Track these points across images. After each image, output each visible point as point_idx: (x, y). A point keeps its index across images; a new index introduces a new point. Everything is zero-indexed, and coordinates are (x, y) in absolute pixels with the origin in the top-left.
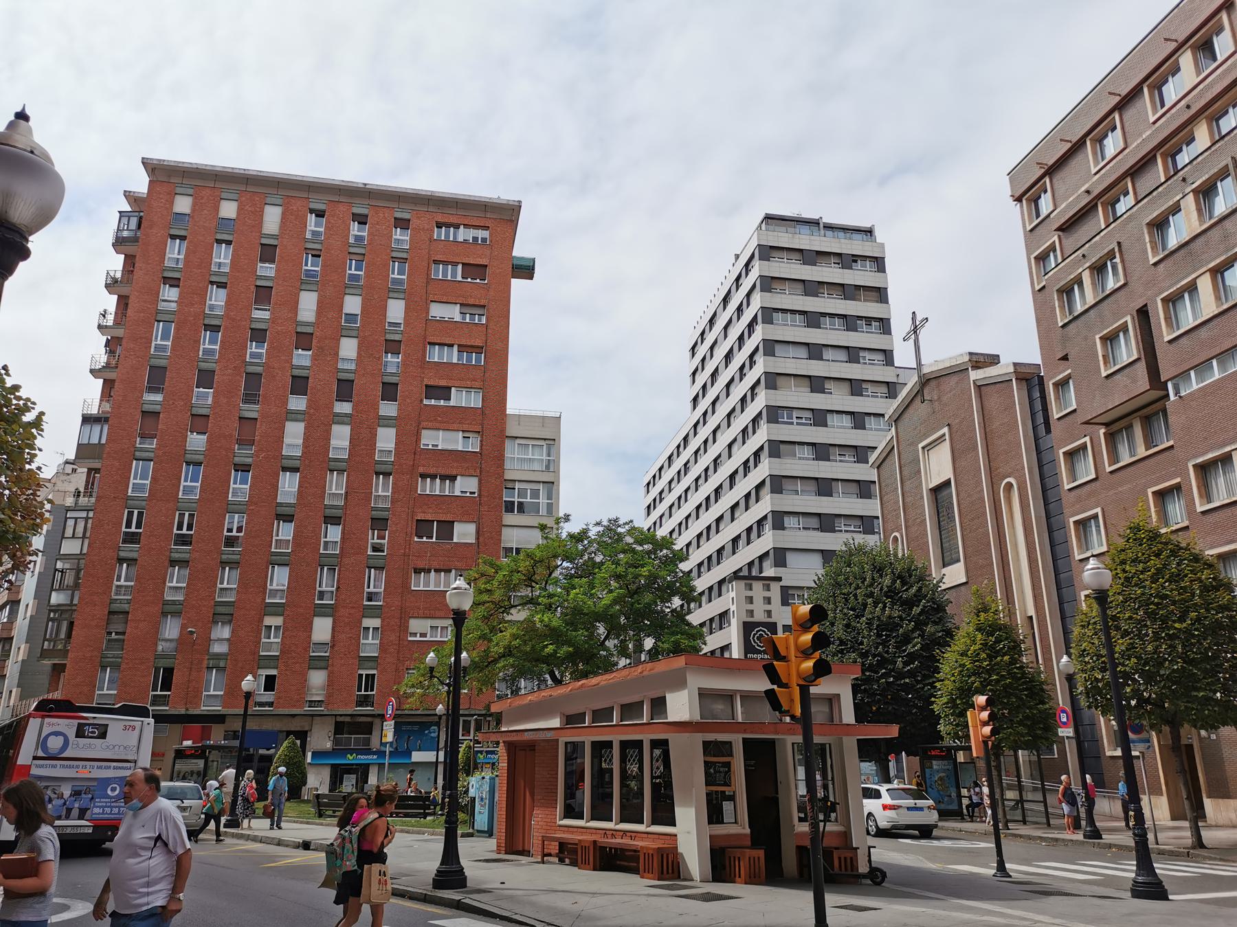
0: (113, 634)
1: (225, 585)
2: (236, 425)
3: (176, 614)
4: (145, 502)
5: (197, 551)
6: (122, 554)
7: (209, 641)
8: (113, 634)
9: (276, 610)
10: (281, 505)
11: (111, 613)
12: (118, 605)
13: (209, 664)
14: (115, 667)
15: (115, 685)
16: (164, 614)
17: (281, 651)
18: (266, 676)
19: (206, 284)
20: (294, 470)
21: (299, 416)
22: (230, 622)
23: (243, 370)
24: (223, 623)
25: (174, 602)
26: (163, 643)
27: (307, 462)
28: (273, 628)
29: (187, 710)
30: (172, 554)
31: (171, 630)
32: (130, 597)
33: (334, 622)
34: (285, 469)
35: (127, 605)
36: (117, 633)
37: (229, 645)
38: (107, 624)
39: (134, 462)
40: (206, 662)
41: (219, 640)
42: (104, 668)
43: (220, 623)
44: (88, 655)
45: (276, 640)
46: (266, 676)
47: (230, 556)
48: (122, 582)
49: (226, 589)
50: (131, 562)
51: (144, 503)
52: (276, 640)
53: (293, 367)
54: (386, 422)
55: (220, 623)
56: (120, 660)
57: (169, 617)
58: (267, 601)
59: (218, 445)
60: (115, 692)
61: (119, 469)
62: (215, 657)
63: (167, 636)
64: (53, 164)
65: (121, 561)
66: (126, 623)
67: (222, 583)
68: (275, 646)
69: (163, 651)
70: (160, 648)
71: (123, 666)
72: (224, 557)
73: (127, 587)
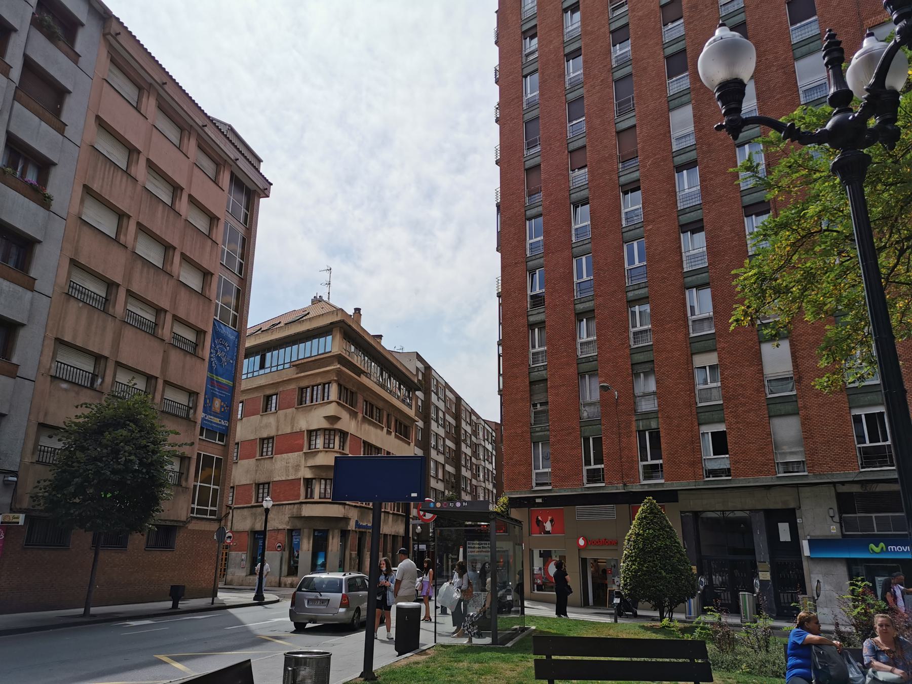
0: (538, 406)
1: (639, 328)
2: (615, 141)
3: (593, 373)
4: (543, 259)
5: (600, 296)
6: (532, 319)
7: (634, 398)
8: (538, 406)
9: (705, 345)
10: (684, 212)
11: (532, 383)
12: (536, 373)
13: (638, 426)
14: (546, 441)
15: (549, 462)
16: (581, 375)
17: (724, 398)
18: (712, 433)
19: (561, 13)
20: (690, 165)
21: (685, 99)
22: (652, 371)
23: (610, 79)
24: (646, 375)
25: (588, 360)
26: (587, 408)
27: (705, 148)
28: (707, 368)
29: (625, 485)
30: (577, 306)
31: (591, 391)
32: (546, 363)
33: (792, 346)
34: (679, 169)
35: (544, 372)
36: (541, 404)
37: (658, 398)
38: (531, 395)
39: (528, 222)
40: (634, 424)
41: (645, 395)
42: (536, 444)
43: (642, 375)
44: (519, 431)
45: (714, 385)
46: (712, 433)
47: (637, 292)
48: (537, 349)
49: (641, 332)
50: (541, 325)
51: (542, 260)
52: (714, 385)
53: (664, 46)
54: (804, 49)
55: (642, 375)
56: (548, 433)
57: (587, 377)
58: (692, 335)
59: (600, 171)
60: (550, 470)
61: (515, 234)
62: (644, 417)
63: (588, 399)
64: (112, 12)
65: (532, 326)
66: (547, 391)
67: (634, 326)
68: (715, 392)
69: (589, 417)
70: (585, 414)
71: (552, 439)
72: (630, 294)
73: (542, 352)
